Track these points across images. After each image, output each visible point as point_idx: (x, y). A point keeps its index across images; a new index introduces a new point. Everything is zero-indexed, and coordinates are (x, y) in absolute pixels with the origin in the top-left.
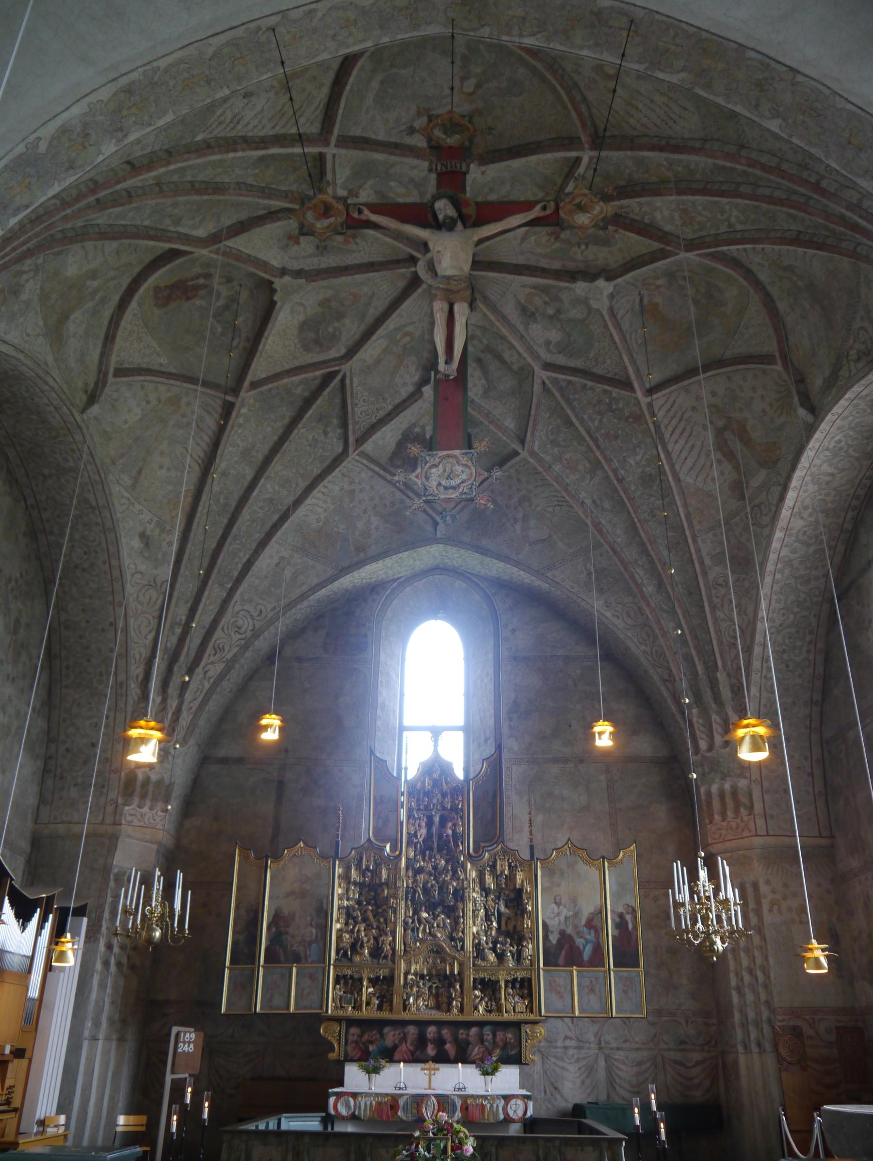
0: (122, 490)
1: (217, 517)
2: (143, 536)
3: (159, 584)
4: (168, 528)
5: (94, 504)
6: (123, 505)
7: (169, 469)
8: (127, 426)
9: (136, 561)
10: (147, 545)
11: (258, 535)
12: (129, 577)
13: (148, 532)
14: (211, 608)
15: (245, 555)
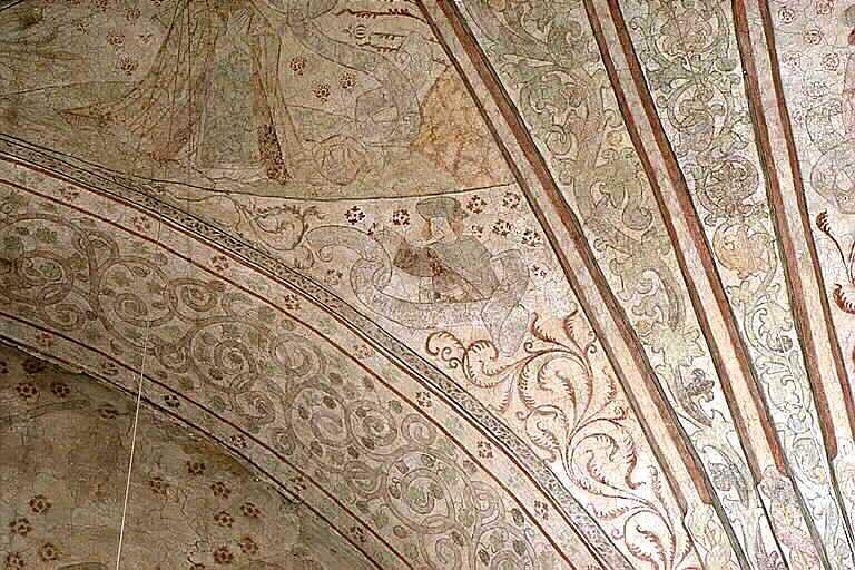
0: (243, 200)
1: (565, 78)
2: (408, 260)
3: (560, 335)
4: (464, 199)
5: (208, 278)
6: (281, 227)
7: (347, 84)
8: (140, 73)
9: (441, 326)
10: (439, 271)
11: (714, 21)
12: (457, 375)
13: (420, 244)
14: (755, 283)
15: (726, 94)
